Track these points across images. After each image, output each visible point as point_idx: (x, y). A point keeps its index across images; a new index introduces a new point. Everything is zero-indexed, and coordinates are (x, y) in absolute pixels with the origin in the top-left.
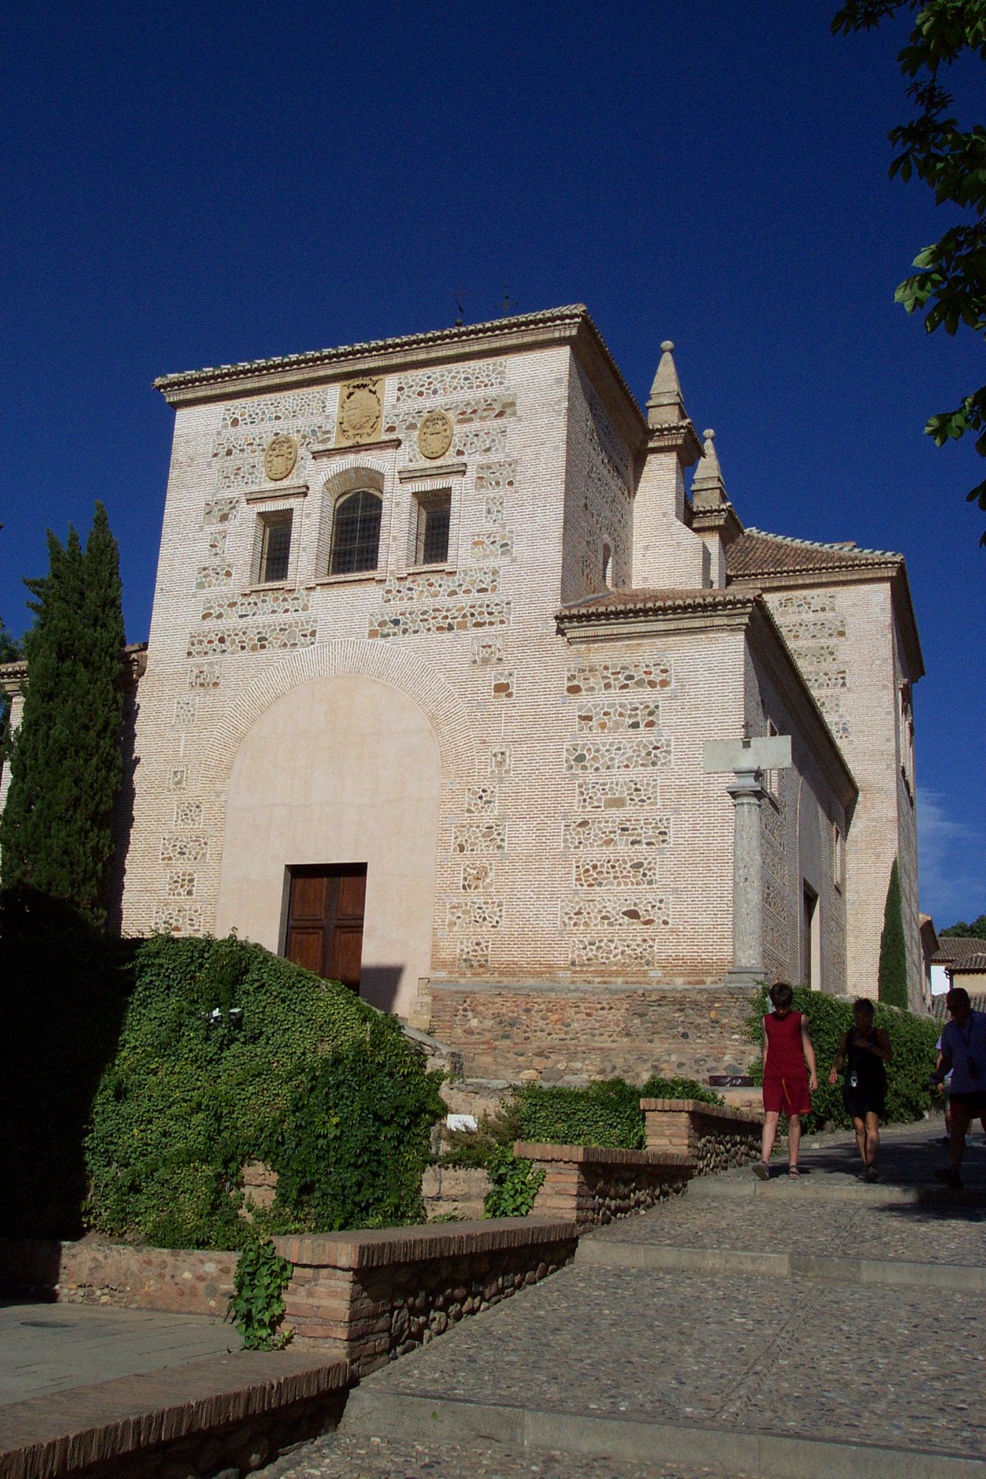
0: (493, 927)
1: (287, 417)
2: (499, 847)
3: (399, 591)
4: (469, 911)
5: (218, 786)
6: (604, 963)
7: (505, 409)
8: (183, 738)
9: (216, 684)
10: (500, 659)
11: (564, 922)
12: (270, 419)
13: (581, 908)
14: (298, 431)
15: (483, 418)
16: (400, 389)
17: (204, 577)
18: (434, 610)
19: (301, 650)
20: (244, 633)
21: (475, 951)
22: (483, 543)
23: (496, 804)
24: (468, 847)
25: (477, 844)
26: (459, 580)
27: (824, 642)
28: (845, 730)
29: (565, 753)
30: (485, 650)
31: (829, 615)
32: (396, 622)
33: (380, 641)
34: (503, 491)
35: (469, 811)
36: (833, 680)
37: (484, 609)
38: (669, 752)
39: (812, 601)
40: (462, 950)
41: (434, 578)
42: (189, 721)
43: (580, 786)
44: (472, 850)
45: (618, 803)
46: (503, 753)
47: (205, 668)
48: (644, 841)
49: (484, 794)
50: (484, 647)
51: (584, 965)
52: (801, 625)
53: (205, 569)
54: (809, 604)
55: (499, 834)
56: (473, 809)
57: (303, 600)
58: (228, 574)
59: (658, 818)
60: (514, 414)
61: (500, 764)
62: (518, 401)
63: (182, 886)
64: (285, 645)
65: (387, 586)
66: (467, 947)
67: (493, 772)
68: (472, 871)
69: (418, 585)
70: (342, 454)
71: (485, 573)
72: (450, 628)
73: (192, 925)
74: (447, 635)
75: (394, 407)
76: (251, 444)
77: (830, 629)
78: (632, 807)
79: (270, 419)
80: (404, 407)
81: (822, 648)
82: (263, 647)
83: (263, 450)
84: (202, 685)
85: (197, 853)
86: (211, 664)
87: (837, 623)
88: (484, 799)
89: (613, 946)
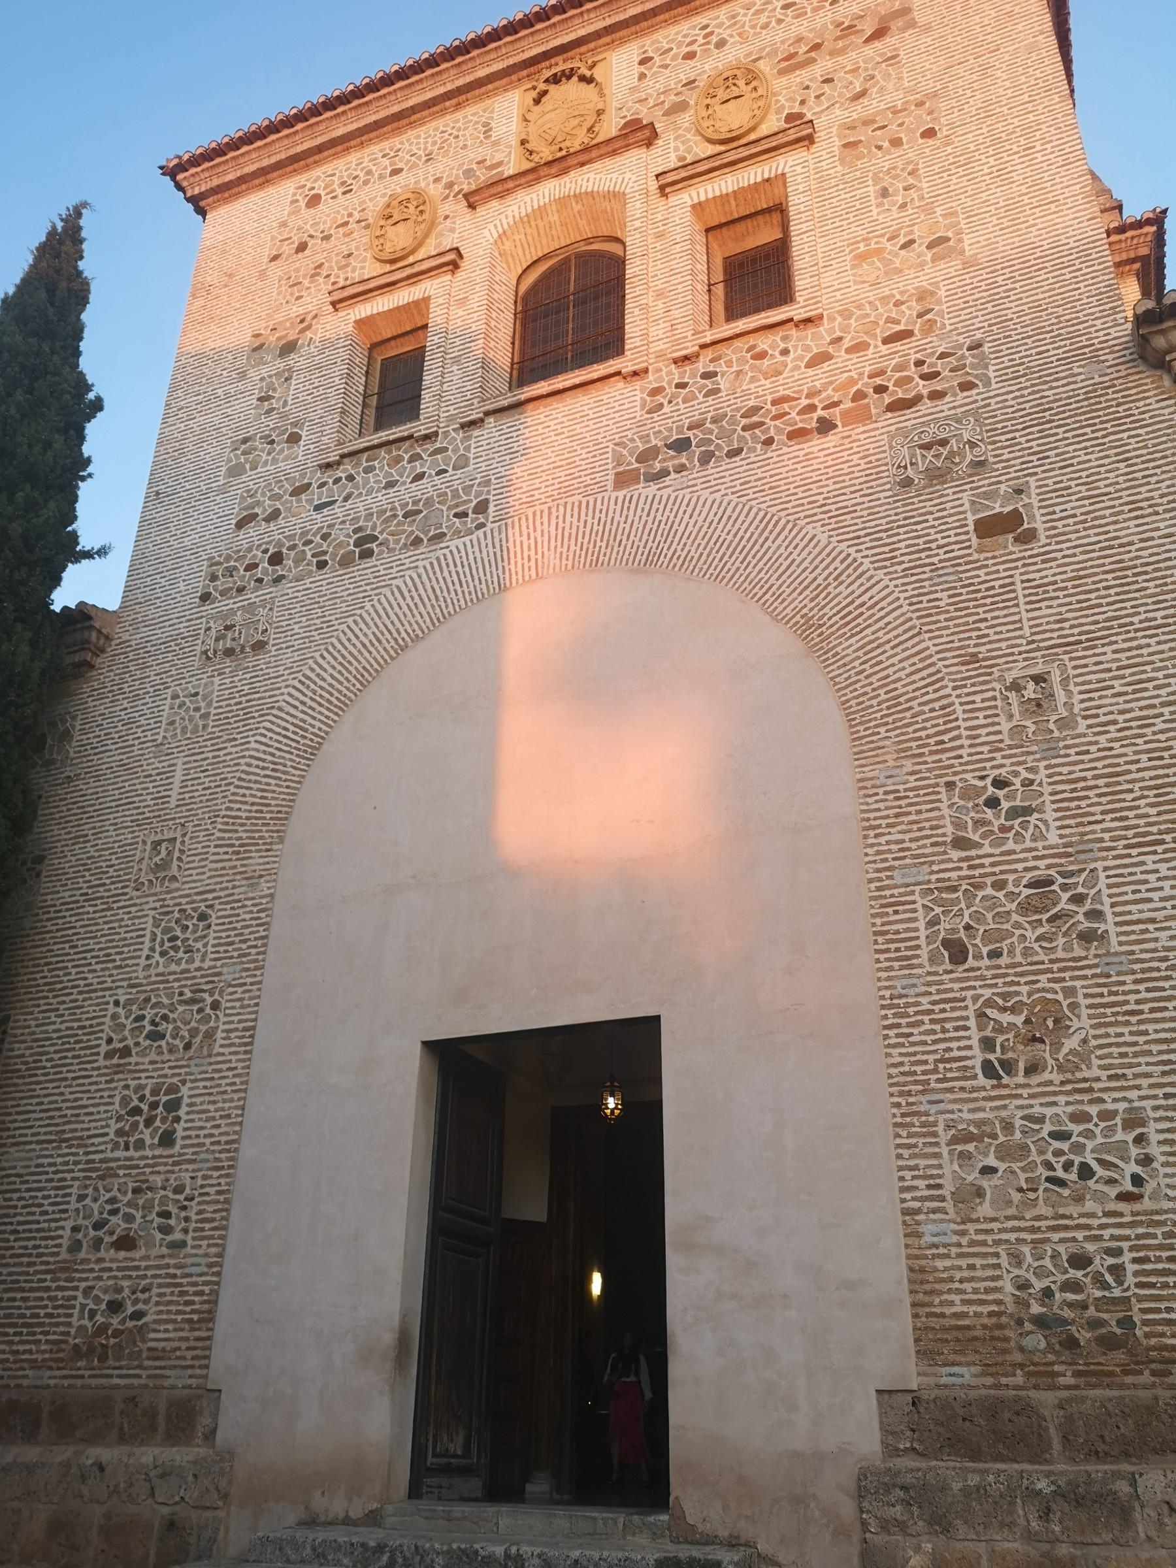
0: (1123, 1197)
1: (415, 166)
2: (1087, 937)
4: (1025, 1148)
5: (256, 862)
8: (180, 767)
9: (259, 646)
12: (381, 177)
14: (437, 180)
16: (642, 62)
17: (244, 453)
18: (774, 403)
19: (453, 544)
20: (325, 537)
21: (1072, 1286)
22: (879, 252)
23: (1050, 815)
24: (977, 944)
25: (1004, 935)
26: (830, 331)
30: (930, 455)
32: (682, 445)
34: (915, 150)
37: (912, 371)
40: (1024, 1286)
41: (763, 342)
42: (195, 730)
44: (995, 954)
46: (1038, 679)
47: (238, 617)
49: (1000, 793)
50: (927, 447)
53: (245, 441)
56: (976, 838)
57: (455, 450)
60: (912, 24)
63: (149, 1122)
64: (417, 542)
65: (651, 381)
66: (1040, 1273)
67: (1017, 730)
68: (1006, 1018)
69: (729, 364)
70: (529, 185)
71: (898, 304)
72: (825, 426)
73: (166, 1230)
74: (816, 445)
75: (633, 90)
76: (346, 224)
79: (381, 177)
82: (367, 554)
83: (367, 227)
84: (229, 652)
85: (194, 1033)
86: (251, 608)
88: (1005, 805)
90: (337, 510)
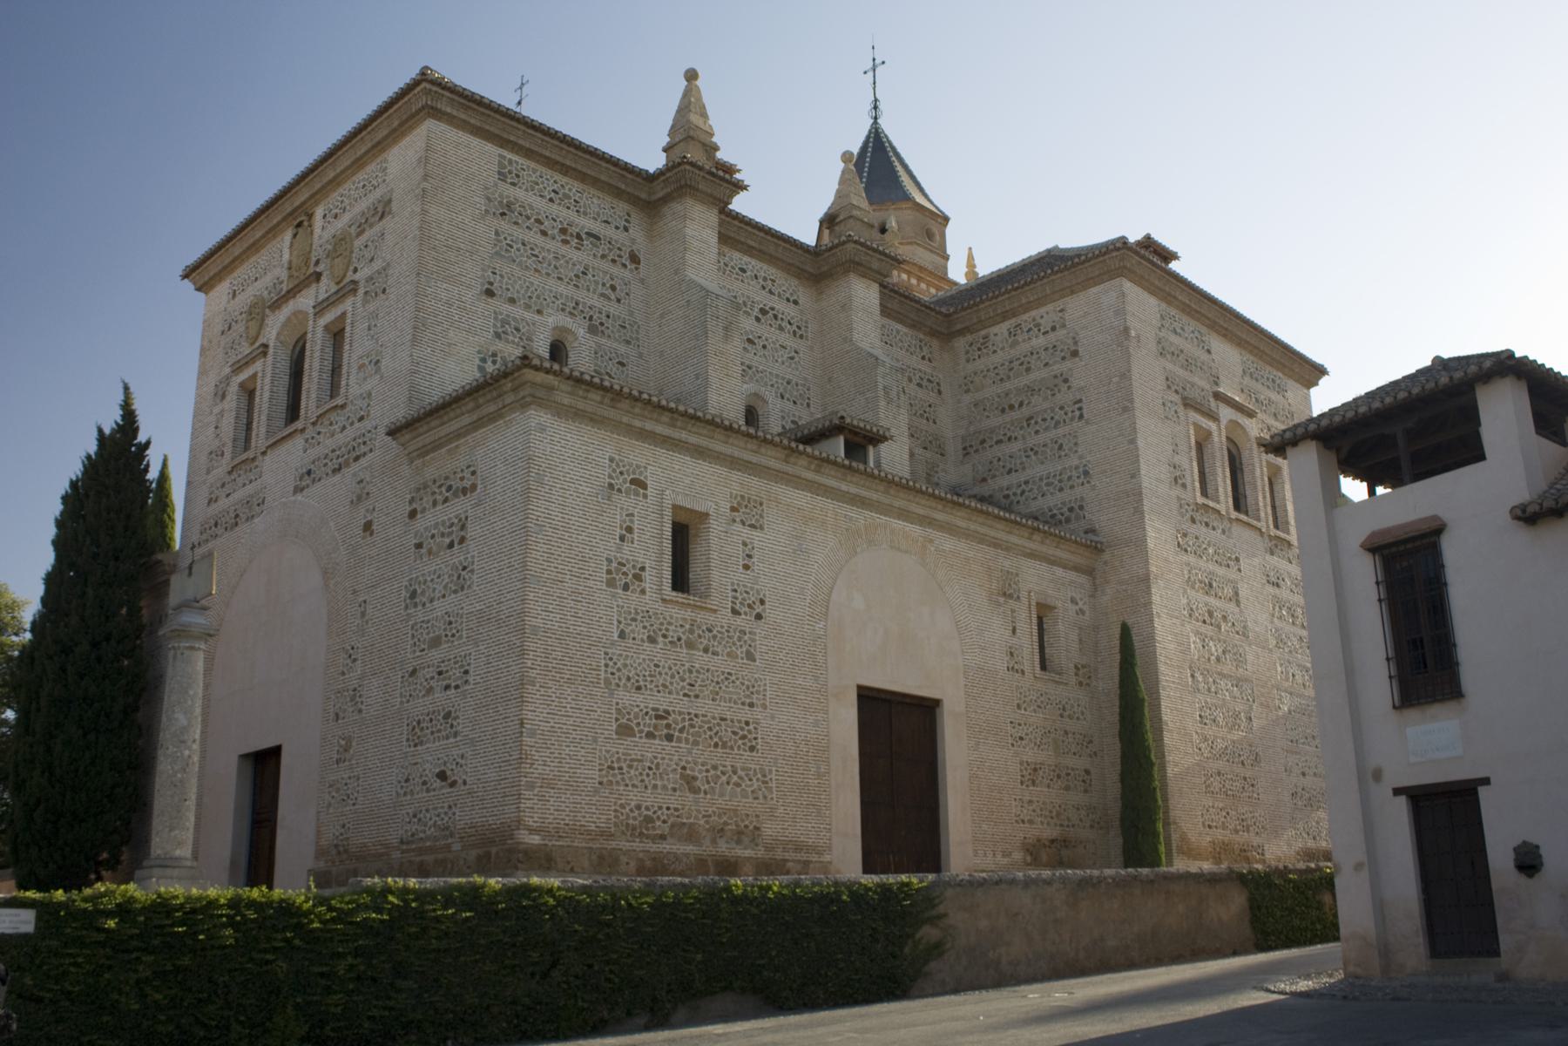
0: (354, 804)
3: (313, 438)
6: (422, 839)
7: (383, 210)
10: (368, 494)
11: (397, 792)
13: (409, 774)
15: (371, 226)
16: (325, 216)
27: (1057, 368)
28: (1086, 473)
29: (403, 592)
31: (1061, 333)
32: (309, 473)
33: (299, 497)
35: (343, 674)
36: (1070, 414)
38: (472, 571)
39: (1042, 321)
43: (412, 628)
45: (435, 642)
46: (365, 602)
48: (453, 684)
50: (359, 483)
51: (408, 843)
52: (1032, 354)
55: (360, 696)
58: (222, 455)
59: (463, 653)
61: (363, 614)
62: (394, 194)
72: (340, 469)
74: (338, 477)
77: (1062, 351)
80: (327, 235)
81: (1056, 377)
82: (237, 524)
89: (428, 816)
90: (231, 498)
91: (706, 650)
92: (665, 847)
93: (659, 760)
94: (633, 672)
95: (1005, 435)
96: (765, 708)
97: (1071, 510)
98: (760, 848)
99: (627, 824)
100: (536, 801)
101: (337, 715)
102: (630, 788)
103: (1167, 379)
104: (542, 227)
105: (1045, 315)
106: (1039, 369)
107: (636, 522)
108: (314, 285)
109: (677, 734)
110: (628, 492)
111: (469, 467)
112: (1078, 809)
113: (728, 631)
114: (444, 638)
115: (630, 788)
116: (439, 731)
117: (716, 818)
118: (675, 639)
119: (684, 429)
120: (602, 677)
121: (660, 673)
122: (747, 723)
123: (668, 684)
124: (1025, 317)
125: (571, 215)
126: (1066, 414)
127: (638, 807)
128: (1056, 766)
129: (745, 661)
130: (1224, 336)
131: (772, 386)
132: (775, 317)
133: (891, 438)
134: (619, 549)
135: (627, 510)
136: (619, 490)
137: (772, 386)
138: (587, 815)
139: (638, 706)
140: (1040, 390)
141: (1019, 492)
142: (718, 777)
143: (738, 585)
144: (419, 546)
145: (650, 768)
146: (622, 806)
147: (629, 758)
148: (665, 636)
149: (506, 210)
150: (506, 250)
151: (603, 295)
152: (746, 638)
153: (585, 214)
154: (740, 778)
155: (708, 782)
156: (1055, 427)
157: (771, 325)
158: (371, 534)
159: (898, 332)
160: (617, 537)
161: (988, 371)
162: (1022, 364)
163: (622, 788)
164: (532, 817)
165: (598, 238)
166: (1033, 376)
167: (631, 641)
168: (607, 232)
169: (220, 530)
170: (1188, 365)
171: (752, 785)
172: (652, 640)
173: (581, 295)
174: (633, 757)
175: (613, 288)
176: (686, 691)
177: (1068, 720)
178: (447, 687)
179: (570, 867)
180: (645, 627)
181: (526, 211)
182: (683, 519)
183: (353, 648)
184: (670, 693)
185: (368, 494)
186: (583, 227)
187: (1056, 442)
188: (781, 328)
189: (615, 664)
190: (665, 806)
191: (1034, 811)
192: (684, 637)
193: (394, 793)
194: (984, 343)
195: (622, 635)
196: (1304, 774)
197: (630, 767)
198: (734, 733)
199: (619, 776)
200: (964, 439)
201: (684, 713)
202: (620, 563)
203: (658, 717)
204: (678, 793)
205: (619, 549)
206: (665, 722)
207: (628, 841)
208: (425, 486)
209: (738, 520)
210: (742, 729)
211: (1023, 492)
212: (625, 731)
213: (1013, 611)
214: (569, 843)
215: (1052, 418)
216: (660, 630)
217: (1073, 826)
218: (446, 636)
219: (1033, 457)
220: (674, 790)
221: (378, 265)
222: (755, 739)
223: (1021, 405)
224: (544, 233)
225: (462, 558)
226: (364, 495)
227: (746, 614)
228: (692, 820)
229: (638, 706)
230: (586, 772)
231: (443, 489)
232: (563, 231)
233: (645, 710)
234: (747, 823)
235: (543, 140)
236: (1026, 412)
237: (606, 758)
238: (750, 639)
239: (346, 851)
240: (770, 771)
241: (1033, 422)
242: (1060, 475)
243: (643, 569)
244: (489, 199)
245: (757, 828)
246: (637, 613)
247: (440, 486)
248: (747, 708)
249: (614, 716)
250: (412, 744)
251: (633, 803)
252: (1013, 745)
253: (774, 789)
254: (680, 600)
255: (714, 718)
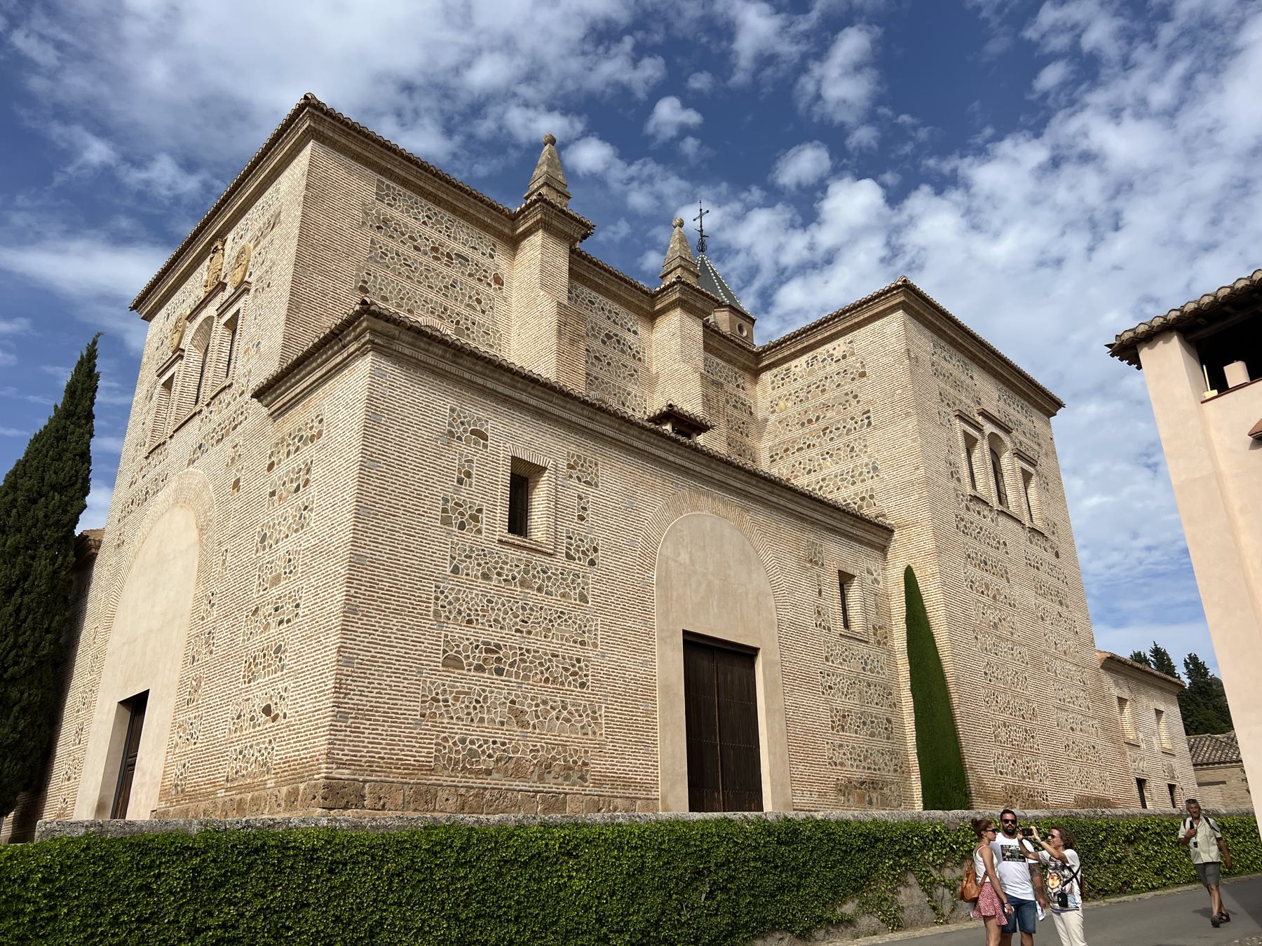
0: (195, 743)
6: (243, 776)
10: (240, 455)
27: (847, 388)
28: (875, 469)
31: (851, 359)
32: (200, 447)
33: (191, 469)
36: (860, 423)
38: (311, 510)
45: (276, 580)
46: (227, 551)
48: (286, 619)
52: (826, 378)
54: (832, 355)
59: (296, 588)
77: (852, 373)
78: (284, 583)
81: (847, 394)
87: (858, 365)
91: (539, 590)
92: (489, 782)
93: (487, 693)
94: (465, 606)
95: (805, 443)
96: (596, 647)
97: (863, 499)
98: (586, 784)
99: (450, 759)
100: (348, 733)
101: (194, 657)
102: (455, 721)
103: (941, 394)
104: (415, 244)
105: (837, 348)
106: (833, 390)
107: (475, 468)
108: (222, 293)
109: (507, 668)
110: (468, 442)
111: (318, 416)
112: (883, 754)
113: (562, 574)
114: (283, 576)
115: (455, 721)
116: (269, 666)
117: (544, 753)
118: (510, 577)
119: (525, 391)
120: (432, 609)
121: (493, 609)
122: (578, 661)
123: (500, 619)
124: (819, 350)
125: (443, 238)
126: (856, 423)
127: (463, 741)
128: (862, 714)
129: (578, 602)
130: (983, 368)
131: (615, 395)
132: (618, 342)
133: (712, 427)
134: (457, 491)
135: (467, 456)
136: (459, 438)
137: (615, 395)
138: (406, 748)
139: (467, 639)
140: (833, 406)
141: (817, 487)
142: (548, 711)
143: (573, 532)
144: (273, 494)
145: (477, 701)
146: (445, 740)
147: (455, 690)
148: (499, 574)
149: (383, 224)
150: (381, 257)
151: (468, 305)
152: (579, 581)
153: (455, 239)
154: (570, 713)
155: (538, 717)
156: (847, 434)
157: (614, 348)
158: (238, 491)
159: (718, 364)
160: (455, 480)
161: (790, 395)
162: (818, 387)
163: (446, 721)
164: (343, 750)
165: (468, 261)
166: (827, 395)
167: (464, 577)
168: (477, 256)
169: (133, 507)
170: (957, 385)
171: (581, 721)
172: (486, 576)
173: (450, 303)
174: (460, 689)
175: (479, 301)
176: (519, 627)
177: (869, 673)
178: (281, 622)
179: (381, 803)
180: (479, 565)
181: (400, 228)
182: (521, 471)
183: (213, 594)
184: (501, 628)
185: (240, 455)
186: (453, 249)
187: (848, 446)
188: (623, 351)
189: (446, 597)
190: (491, 740)
191: (844, 754)
192: (519, 577)
193: (227, 730)
194: (787, 374)
195: (455, 570)
196: (1072, 729)
197: (456, 699)
198: (566, 670)
199: (444, 709)
200: (771, 449)
201: (515, 648)
202: (456, 504)
203: (488, 651)
204: (504, 728)
205: (457, 491)
206: (497, 655)
207: (450, 776)
208: (283, 440)
209: (574, 476)
210: (573, 666)
211: (821, 487)
212: (452, 662)
213: (818, 576)
214: (383, 778)
215: (844, 427)
216: (495, 568)
217: (879, 769)
218: (285, 573)
219: (829, 459)
220: (502, 723)
221: (268, 263)
222: (586, 675)
223: (818, 418)
224: (417, 248)
225: (304, 499)
226: (237, 457)
227: (580, 559)
228: (519, 755)
229: (467, 639)
230: (408, 703)
231: (296, 440)
232: (435, 249)
233: (475, 643)
234: (575, 758)
235: (417, 172)
236: (822, 424)
237: (430, 690)
238: (583, 582)
239: (183, 791)
240: (600, 707)
241: (828, 431)
242: (852, 472)
243: (480, 511)
244: (366, 213)
245: (585, 764)
246: (472, 551)
247: (294, 438)
248: (579, 646)
249: (442, 648)
250: (247, 680)
251: (457, 737)
252: (823, 693)
253: (604, 726)
254: (517, 542)
255: (546, 654)
